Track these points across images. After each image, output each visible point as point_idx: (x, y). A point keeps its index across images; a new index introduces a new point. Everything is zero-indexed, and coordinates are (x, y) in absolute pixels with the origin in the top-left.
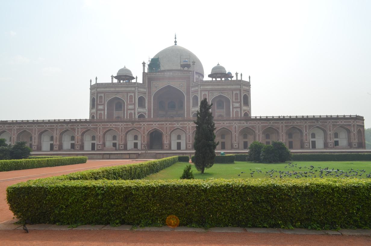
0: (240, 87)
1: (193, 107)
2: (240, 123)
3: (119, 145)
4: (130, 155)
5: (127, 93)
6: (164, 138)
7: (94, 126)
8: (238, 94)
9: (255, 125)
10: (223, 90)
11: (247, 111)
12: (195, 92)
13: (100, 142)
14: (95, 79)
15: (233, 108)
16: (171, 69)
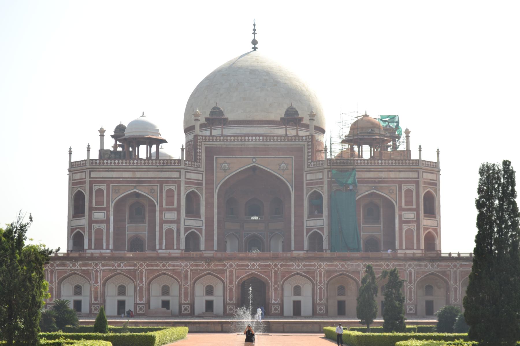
0: (417, 177)
1: (309, 217)
2: (420, 266)
3: (180, 305)
4: (224, 325)
5: (162, 183)
6: (270, 293)
7: (130, 266)
8: (412, 191)
9: (449, 269)
10: (379, 182)
11: (433, 229)
12: (317, 183)
13: (141, 299)
14: (87, 149)
15: (401, 222)
16: (250, 119)
